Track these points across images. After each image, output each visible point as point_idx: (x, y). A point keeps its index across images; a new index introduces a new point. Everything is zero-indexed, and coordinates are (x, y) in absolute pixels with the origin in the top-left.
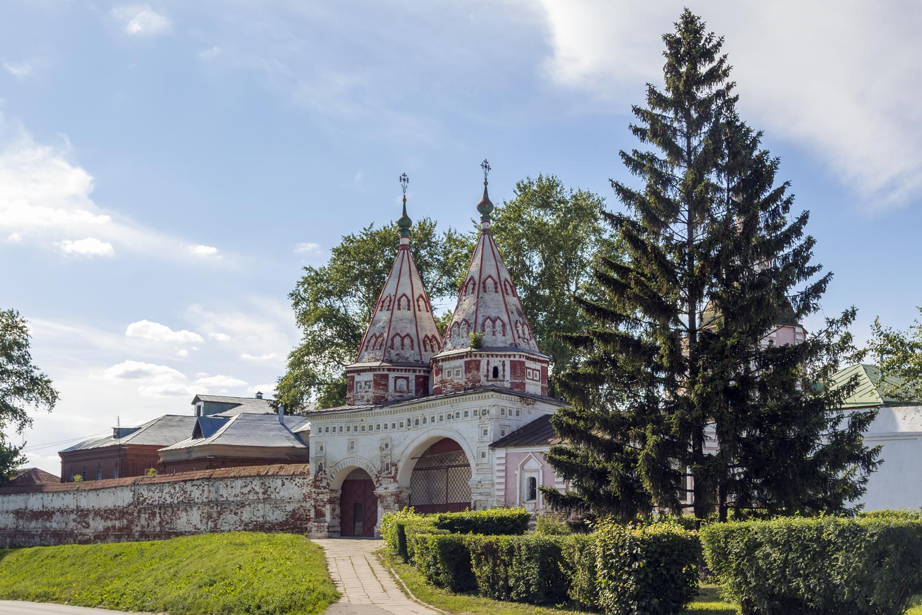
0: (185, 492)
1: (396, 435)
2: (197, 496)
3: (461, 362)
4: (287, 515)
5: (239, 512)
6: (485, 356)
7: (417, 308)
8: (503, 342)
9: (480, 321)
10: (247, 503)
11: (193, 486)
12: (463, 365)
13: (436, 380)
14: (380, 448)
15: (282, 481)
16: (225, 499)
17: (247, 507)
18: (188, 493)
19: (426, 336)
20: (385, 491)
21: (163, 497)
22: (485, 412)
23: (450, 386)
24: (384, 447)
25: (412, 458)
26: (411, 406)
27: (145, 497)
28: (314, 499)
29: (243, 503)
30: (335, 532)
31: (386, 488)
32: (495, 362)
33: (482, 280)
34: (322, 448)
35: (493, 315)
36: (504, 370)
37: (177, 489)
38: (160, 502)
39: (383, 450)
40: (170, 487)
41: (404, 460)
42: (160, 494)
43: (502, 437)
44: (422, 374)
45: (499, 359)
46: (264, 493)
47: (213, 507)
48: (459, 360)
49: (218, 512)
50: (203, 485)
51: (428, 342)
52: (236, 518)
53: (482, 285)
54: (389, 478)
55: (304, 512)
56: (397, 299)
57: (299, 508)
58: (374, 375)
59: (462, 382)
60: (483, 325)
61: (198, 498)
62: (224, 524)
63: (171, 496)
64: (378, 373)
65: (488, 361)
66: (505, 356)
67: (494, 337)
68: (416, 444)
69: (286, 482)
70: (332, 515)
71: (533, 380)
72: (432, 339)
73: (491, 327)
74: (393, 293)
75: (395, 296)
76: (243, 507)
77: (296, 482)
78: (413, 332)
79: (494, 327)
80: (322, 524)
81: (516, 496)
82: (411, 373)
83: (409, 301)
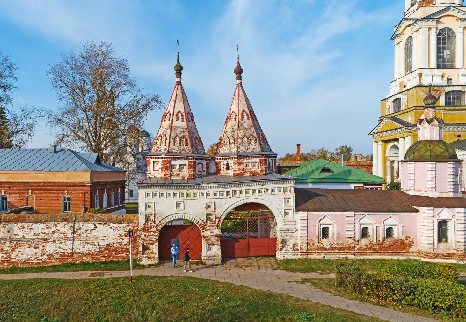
1: (219, 201)
4: (100, 248)
5: (41, 246)
12: (259, 161)
14: (206, 208)
17: (51, 243)
20: (211, 234)
28: (143, 239)
29: (46, 240)
31: (211, 232)
49: (12, 247)
52: (36, 251)
57: (114, 244)
58: (189, 162)
62: (20, 255)
69: (99, 226)
76: (45, 242)
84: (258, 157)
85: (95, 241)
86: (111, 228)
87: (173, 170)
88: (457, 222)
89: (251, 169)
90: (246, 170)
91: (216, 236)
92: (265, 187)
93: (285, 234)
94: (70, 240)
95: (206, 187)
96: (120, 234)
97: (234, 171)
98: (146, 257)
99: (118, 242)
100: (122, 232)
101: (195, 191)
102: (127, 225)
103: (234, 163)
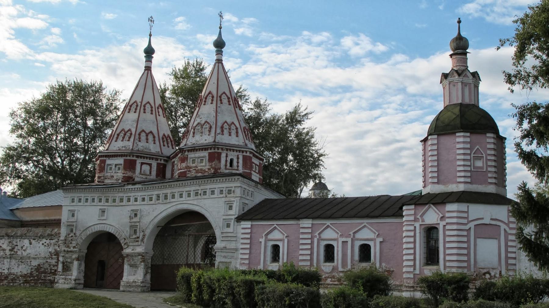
3: (205, 154)
4: (32, 269)
6: (225, 150)
7: (157, 113)
8: (236, 141)
9: (219, 124)
13: (179, 167)
14: (130, 217)
15: (30, 241)
19: (164, 135)
22: (230, 192)
23: (194, 171)
24: (133, 216)
25: (158, 227)
26: (161, 185)
30: (80, 284)
32: (232, 155)
33: (219, 95)
34: (73, 215)
35: (229, 121)
36: (238, 163)
39: (132, 218)
41: (151, 227)
43: (243, 212)
44: (162, 162)
45: (235, 153)
46: (11, 250)
48: (204, 151)
51: (165, 139)
53: (219, 99)
54: (137, 241)
55: (50, 266)
56: (143, 104)
57: (44, 264)
59: (206, 168)
60: (222, 127)
64: (128, 158)
65: (227, 154)
66: (240, 151)
67: (230, 137)
68: (164, 214)
69: (33, 242)
70: (79, 270)
71: (255, 172)
72: (167, 137)
73: (228, 129)
74: (139, 100)
75: (141, 103)
77: (43, 242)
78: (155, 131)
79: (230, 129)
80: (70, 277)
81: (260, 259)
82: (154, 161)
83: (152, 107)
84: (206, 149)
85: (28, 260)
86: (43, 244)
87: (109, 171)
88: (448, 227)
89: (196, 167)
90: (191, 168)
91: (139, 254)
92: (202, 187)
93: (223, 254)
94: (7, 258)
95: (132, 188)
96: (50, 252)
98: (63, 279)
99: (47, 262)
100: (51, 249)
101: (121, 195)
102: (57, 240)
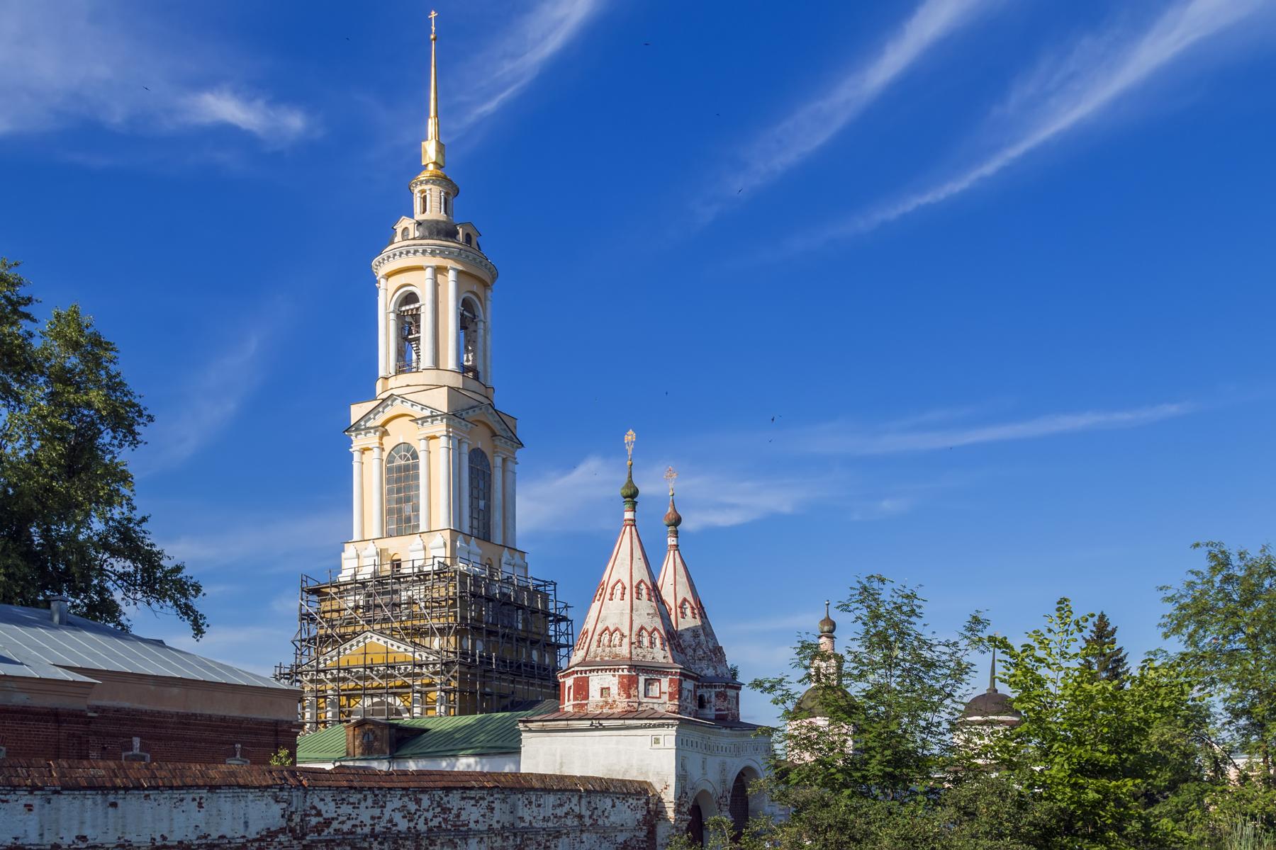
0: (446, 810)
2: (473, 818)
5: (553, 846)
10: (565, 831)
11: (463, 799)
15: (613, 800)
16: (527, 825)
18: (454, 811)
21: (386, 817)
27: (326, 816)
29: (558, 832)
37: (426, 802)
38: (377, 829)
40: (406, 799)
42: (377, 812)
47: (507, 837)
50: (491, 799)
55: (638, 843)
57: (631, 839)
61: (477, 822)
63: (410, 816)
76: (557, 837)
77: (629, 804)
97: (717, 710)
103: (717, 696)
